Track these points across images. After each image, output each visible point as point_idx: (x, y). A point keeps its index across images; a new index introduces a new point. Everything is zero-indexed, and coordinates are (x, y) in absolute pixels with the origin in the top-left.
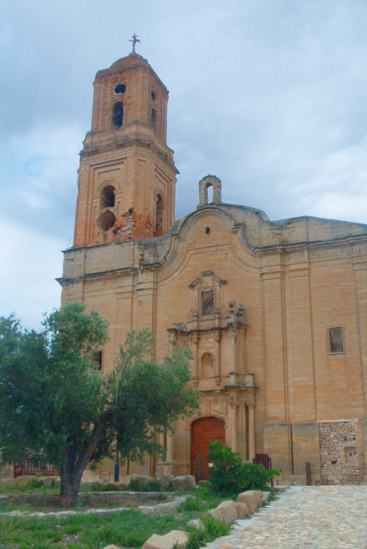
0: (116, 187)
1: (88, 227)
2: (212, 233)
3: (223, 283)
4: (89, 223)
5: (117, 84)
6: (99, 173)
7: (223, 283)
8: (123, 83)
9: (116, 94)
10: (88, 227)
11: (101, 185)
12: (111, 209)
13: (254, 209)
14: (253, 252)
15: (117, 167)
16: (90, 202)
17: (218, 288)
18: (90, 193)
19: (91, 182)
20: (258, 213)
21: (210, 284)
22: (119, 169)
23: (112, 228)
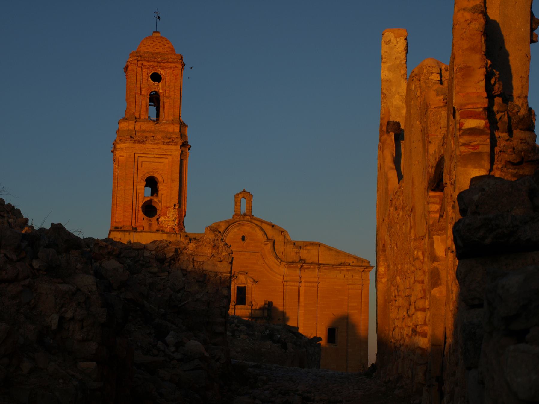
0: (160, 178)
1: (134, 211)
2: (247, 240)
3: (255, 282)
4: (134, 207)
5: (153, 72)
6: (142, 162)
7: (255, 282)
8: (159, 73)
9: (152, 82)
10: (134, 211)
11: (144, 175)
12: (155, 200)
13: (280, 228)
14: (279, 263)
15: (161, 160)
16: (135, 188)
17: (250, 285)
18: (135, 179)
19: (136, 169)
20: (282, 231)
21: (244, 281)
22: (163, 163)
23: (156, 217)
